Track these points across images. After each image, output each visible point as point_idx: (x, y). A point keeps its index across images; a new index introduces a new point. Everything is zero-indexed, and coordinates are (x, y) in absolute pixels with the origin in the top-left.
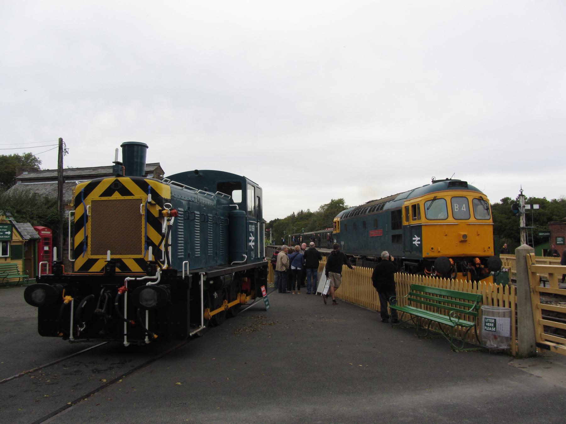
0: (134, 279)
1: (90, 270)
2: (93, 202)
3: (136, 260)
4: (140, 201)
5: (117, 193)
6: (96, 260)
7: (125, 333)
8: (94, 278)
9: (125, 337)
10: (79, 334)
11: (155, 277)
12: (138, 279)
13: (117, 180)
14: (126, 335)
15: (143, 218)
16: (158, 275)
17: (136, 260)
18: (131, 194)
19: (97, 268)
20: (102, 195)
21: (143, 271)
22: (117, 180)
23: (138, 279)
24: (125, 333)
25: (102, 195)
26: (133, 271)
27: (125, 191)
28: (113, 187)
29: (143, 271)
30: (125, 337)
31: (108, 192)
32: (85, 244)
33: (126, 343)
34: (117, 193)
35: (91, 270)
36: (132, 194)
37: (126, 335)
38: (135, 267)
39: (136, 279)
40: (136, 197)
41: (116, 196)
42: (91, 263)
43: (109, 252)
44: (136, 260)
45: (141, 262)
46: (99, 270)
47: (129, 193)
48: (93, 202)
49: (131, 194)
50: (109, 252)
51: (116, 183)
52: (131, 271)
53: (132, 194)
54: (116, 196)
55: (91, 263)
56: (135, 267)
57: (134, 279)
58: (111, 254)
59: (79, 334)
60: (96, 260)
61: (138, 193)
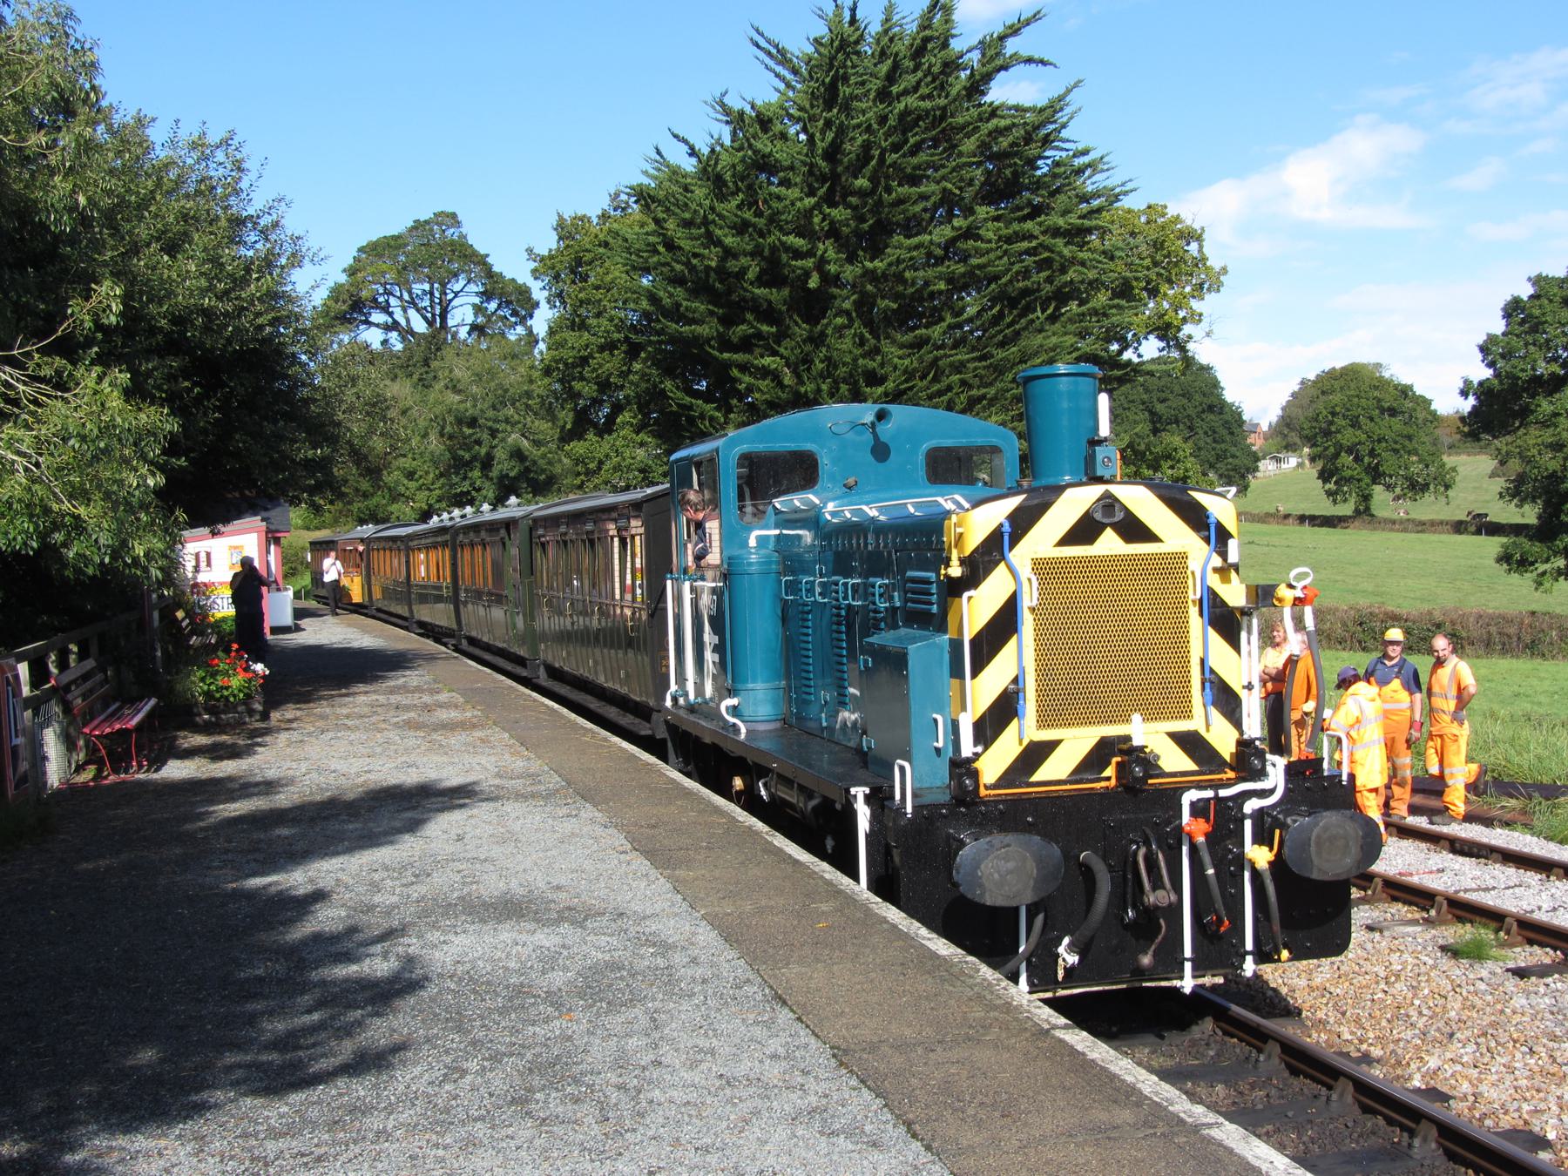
0: (1209, 794)
1: (1036, 778)
2: (1039, 566)
4: (1183, 557)
7: (1188, 953)
10: (1061, 974)
13: (1107, 495)
19: (1056, 768)
22: (1107, 495)
23: (1223, 793)
24: (1188, 953)
27: (1134, 530)
28: (1098, 516)
29: (1194, 767)
31: (1084, 531)
32: (1021, 694)
35: (1039, 776)
37: (1188, 960)
38: (1174, 760)
39: (1216, 797)
41: (1109, 543)
42: (1036, 754)
45: (1191, 743)
46: (1063, 775)
48: (1039, 566)
54: (1109, 543)
55: (1036, 754)
56: (1174, 760)
57: (1209, 794)
59: (1061, 974)
61: (1173, 533)
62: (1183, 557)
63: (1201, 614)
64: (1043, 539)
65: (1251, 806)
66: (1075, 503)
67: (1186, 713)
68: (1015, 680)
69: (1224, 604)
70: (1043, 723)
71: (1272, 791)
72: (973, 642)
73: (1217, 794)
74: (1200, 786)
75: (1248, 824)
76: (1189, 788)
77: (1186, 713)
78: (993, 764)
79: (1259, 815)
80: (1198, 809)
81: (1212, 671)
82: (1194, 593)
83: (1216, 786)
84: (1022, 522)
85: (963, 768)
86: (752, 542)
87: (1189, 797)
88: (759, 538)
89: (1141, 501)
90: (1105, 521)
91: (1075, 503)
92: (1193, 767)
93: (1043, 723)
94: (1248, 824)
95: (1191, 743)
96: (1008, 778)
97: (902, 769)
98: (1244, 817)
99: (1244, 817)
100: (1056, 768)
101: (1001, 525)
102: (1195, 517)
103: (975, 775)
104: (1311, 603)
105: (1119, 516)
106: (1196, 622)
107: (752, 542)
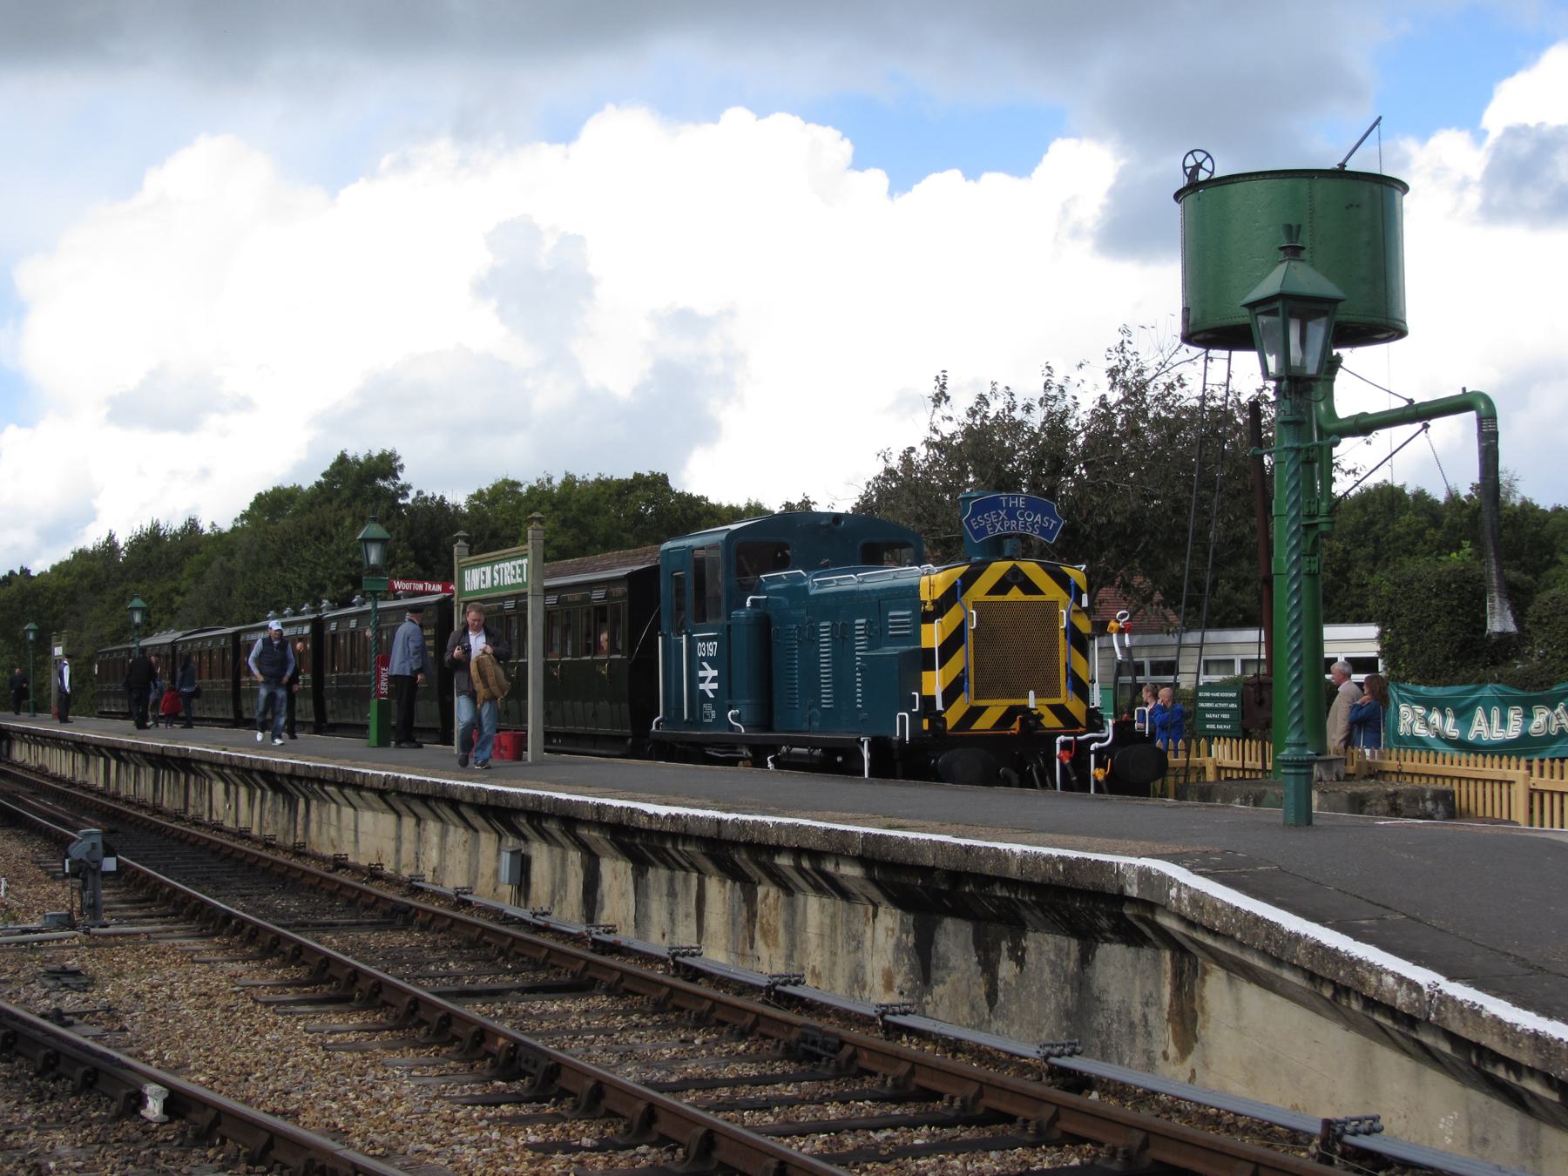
6: (984, 709)
8: (982, 739)
11: (1105, 735)
12: (1079, 738)
15: (1062, 634)
16: (1109, 731)
17: (1052, 708)
19: (984, 723)
20: (989, 593)
23: (1079, 738)
25: (990, 593)
26: (1047, 726)
27: (1029, 587)
28: (1009, 579)
31: (1001, 587)
34: (1015, 588)
36: (1041, 593)
38: (1051, 721)
40: (1049, 597)
41: (1015, 594)
42: (974, 713)
43: (1031, 693)
44: (1052, 708)
45: (1059, 710)
46: (989, 727)
48: (976, 605)
50: (1031, 693)
53: (1041, 593)
54: (1015, 594)
55: (974, 713)
56: (1051, 721)
60: (984, 709)
61: (1052, 591)
63: (1066, 638)
64: (980, 590)
66: (999, 568)
67: (1058, 695)
68: (963, 671)
69: (1079, 631)
70: (977, 697)
71: (1107, 738)
72: (939, 648)
73: (1076, 739)
74: (1066, 735)
75: (1092, 756)
77: (1058, 695)
78: (953, 716)
79: (1098, 752)
80: (1064, 745)
81: (1072, 671)
82: (1063, 625)
83: (1076, 735)
84: (968, 580)
85: (937, 718)
86: (748, 603)
87: (1062, 738)
88: (751, 600)
89: (1031, 568)
91: (999, 568)
92: (1061, 725)
93: (977, 697)
94: (1092, 756)
95: (1059, 710)
96: (958, 726)
97: (902, 718)
98: (1091, 752)
99: (1091, 752)
100: (984, 723)
101: (956, 582)
102: (1063, 581)
103: (944, 720)
105: (1020, 579)
106: (1063, 643)
107: (748, 603)
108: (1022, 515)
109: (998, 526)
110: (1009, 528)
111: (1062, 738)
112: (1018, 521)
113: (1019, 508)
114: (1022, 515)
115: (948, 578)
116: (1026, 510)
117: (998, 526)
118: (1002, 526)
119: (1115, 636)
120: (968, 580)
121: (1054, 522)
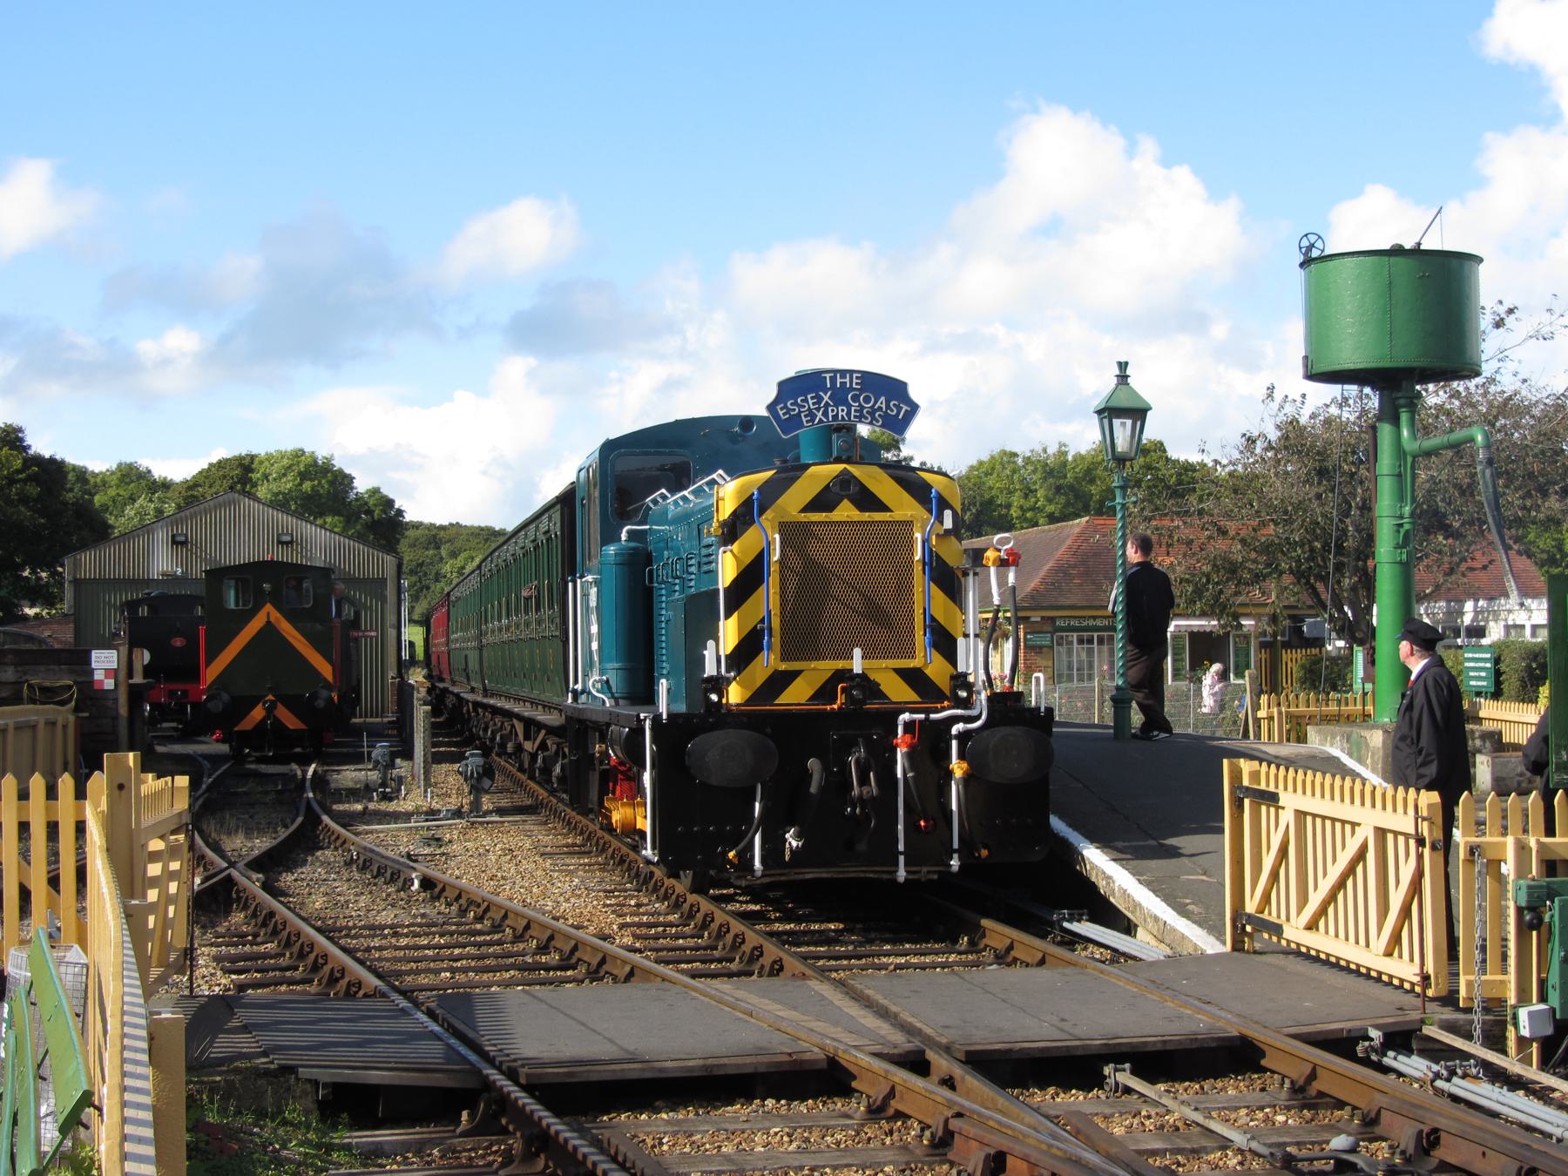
1: (776, 702)
3: (899, 672)
4: (908, 524)
5: (846, 503)
7: (901, 847)
8: (790, 718)
9: (902, 859)
11: (974, 713)
12: (933, 716)
14: (901, 853)
15: (918, 568)
18: (883, 508)
19: (797, 695)
21: (919, 700)
23: (933, 716)
24: (901, 847)
26: (894, 700)
27: (867, 501)
30: (902, 859)
31: (823, 501)
33: (902, 874)
34: (846, 503)
36: (885, 508)
38: (897, 690)
39: (927, 719)
40: (898, 515)
41: (846, 511)
42: (780, 681)
43: (857, 652)
44: (899, 672)
45: (914, 678)
47: (878, 505)
49: (883, 508)
50: (857, 652)
51: (845, 480)
52: (889, 699)
53: (885, 508)
54: (846, 511)
55: (780, 681)
56: (897, 690)
57: (922, 716)
58: (864, 657)
62: (908, 524)
65: (957, 728)
71: (978, 717)
74: (913, 711)
75: (954, 743)
76: (904, 712)
79: (963, 737)
80: (909, 726)
84: (769, 495)
87: (905, 717)
90: (843, 493)
93: (785, 657)
94: (954, 743)
95: (914, 678)
104: (1015, 563)
106: (919, 578)
108: (856, 398)
109: (819, 415)
110: (835, 417)
111: (905, 717)
112: (849, 407)
113: (851, 389)
114: (856, 398)
115: (740, 491)
116: (861, 391)
117: (819, 415)
118: (825, 414)
119: (993, 570)
120: (769, 495)
121: (905, 408)
